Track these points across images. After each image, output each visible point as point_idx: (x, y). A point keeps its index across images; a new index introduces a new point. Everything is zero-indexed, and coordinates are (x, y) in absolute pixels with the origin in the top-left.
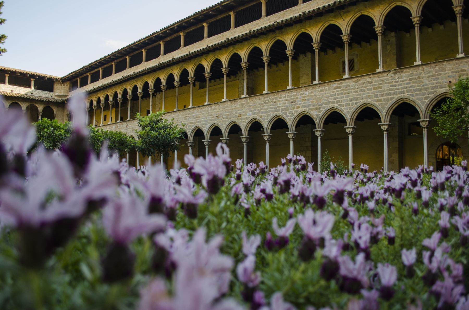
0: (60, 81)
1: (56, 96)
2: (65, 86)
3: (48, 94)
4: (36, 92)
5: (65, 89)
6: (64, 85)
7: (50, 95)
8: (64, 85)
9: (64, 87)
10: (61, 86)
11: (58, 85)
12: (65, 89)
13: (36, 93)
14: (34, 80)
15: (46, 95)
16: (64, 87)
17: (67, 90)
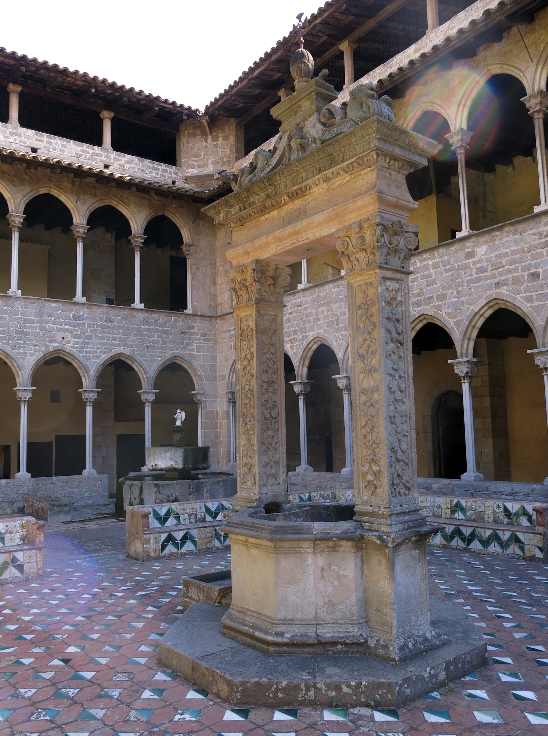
0: (204, 121)
1: (187, 179)
2: (220, 139)
3: (160, 172)
4: (123, 162)
5: (220, 150)
6: (215, 139)
7: (166, 175)
8: (215, 139)
9: (216, 146)
10: (206, 141)
11: (192, 140)
12: (220, 150)
13: (120, 165)
14: (112, 115)
15: (154, 174)
16: (216, 146)
17: (228, 153)
